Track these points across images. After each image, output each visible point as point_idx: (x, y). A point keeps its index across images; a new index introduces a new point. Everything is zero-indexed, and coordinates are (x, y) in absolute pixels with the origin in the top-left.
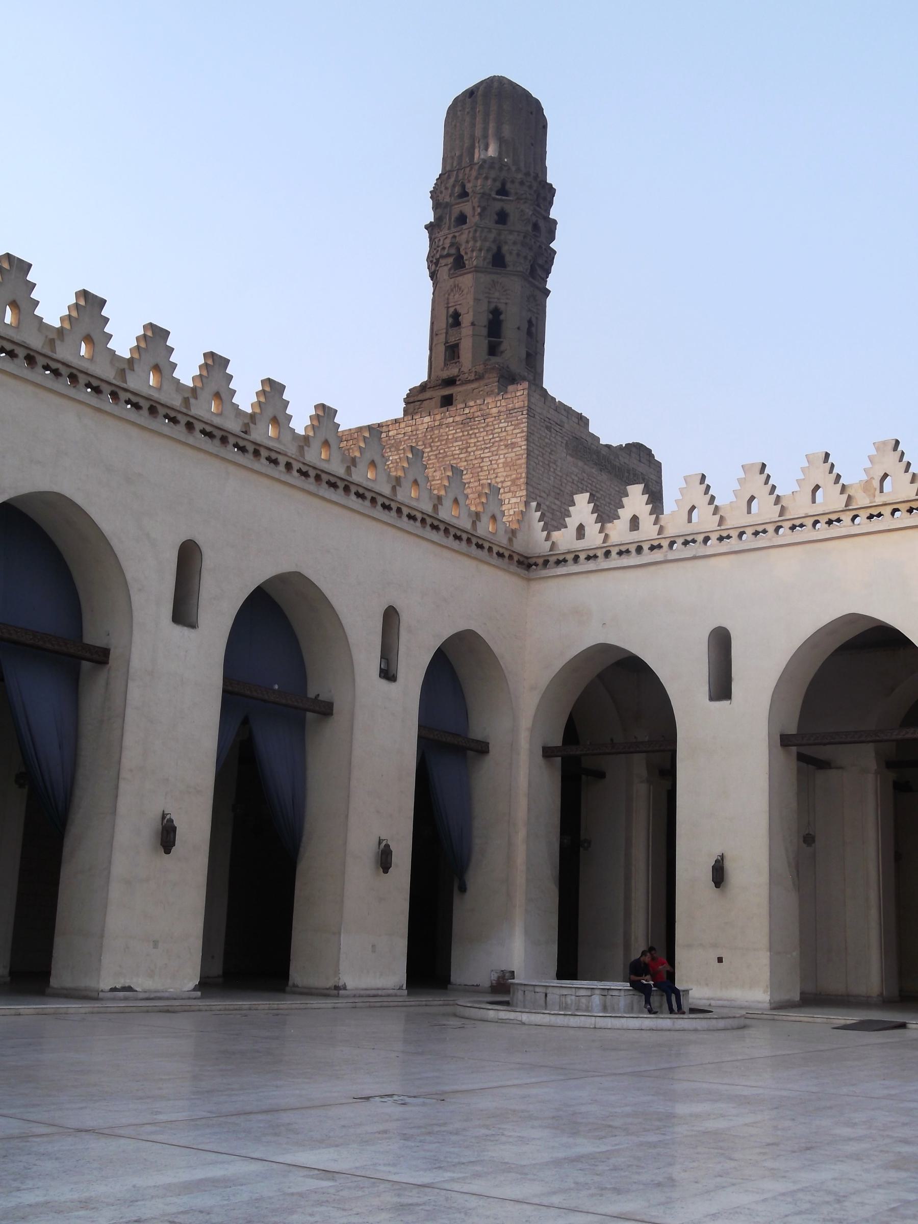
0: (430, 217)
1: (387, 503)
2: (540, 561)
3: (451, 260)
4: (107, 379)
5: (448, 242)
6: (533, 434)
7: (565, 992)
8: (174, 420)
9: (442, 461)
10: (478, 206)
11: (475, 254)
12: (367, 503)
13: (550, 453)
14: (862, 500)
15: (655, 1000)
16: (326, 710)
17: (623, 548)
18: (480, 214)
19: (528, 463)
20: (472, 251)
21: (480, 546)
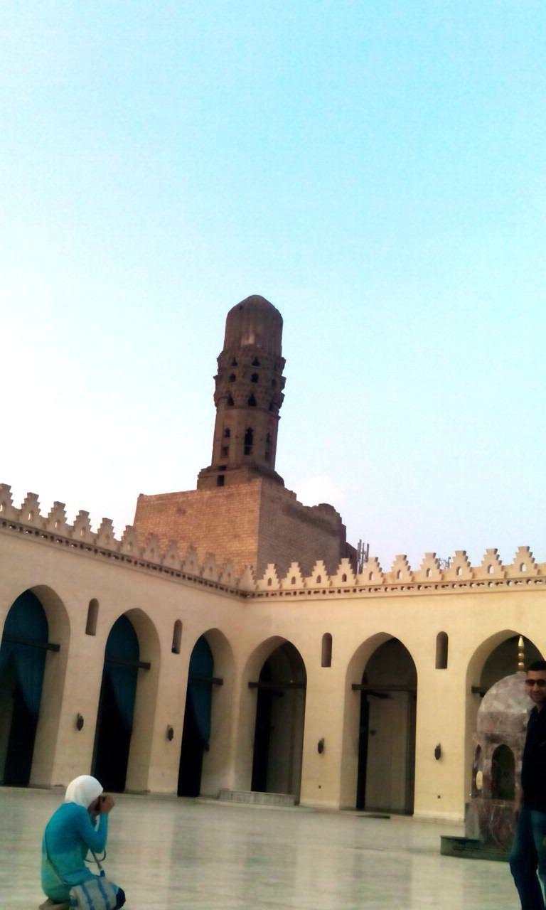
3: (226, 400)
5: (225, 390)
18: (243, 377)
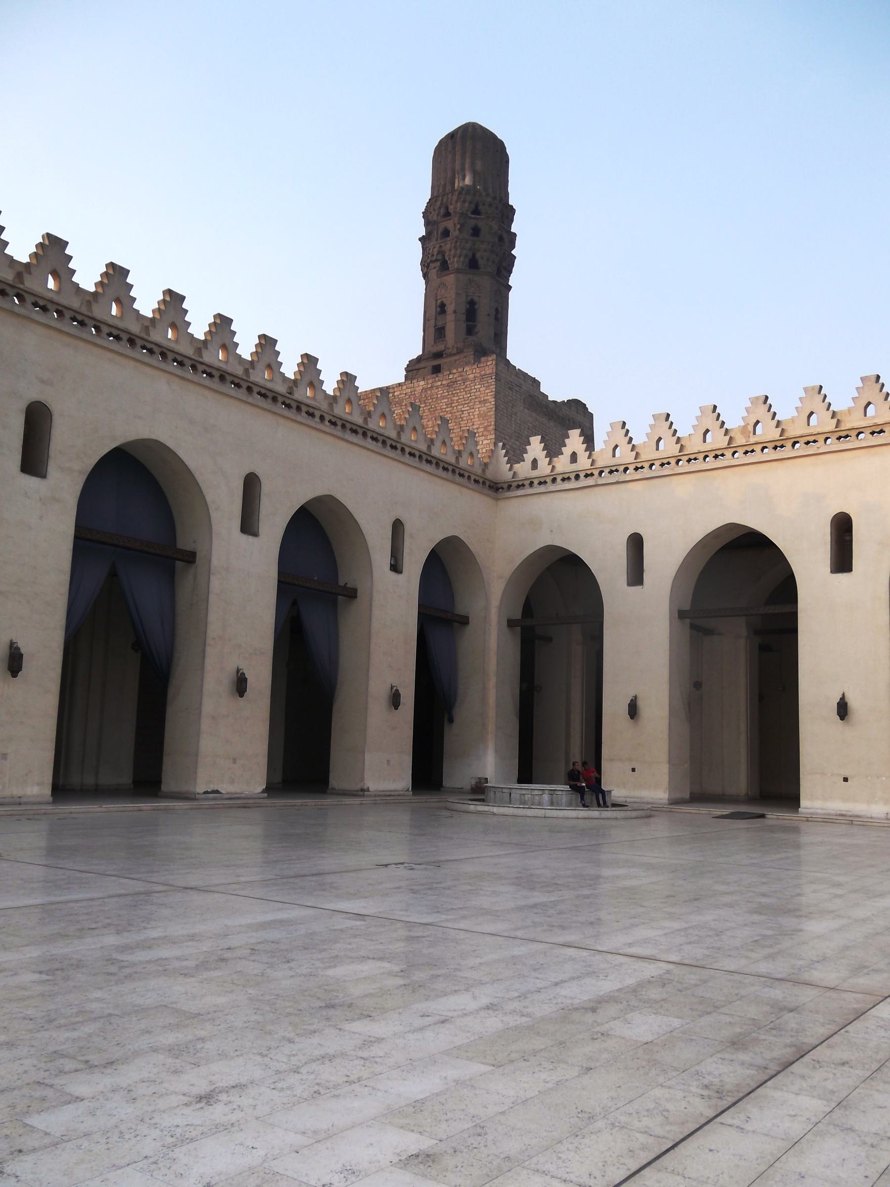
0: (422, 232)
1: (394, 444)
2: (505, 486)
3: (438, 264)
4: (188, 356)
5: (436, 250)
6: (500, 393)
7: (524, 792)
8: (238, 385)
9: (433, 414)
10: (459, 223)
11: (456, 259)
12: (380, 444)
13: (512, 407)
14: (740, 440)
15: (588, 797)
16: (352, 594)
17: (566, 476)
18: (459, 230)
19: (496, 414)
20: (454, 257)
21: (462, 475)
